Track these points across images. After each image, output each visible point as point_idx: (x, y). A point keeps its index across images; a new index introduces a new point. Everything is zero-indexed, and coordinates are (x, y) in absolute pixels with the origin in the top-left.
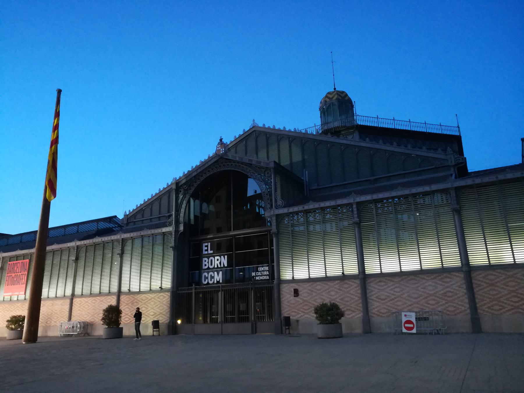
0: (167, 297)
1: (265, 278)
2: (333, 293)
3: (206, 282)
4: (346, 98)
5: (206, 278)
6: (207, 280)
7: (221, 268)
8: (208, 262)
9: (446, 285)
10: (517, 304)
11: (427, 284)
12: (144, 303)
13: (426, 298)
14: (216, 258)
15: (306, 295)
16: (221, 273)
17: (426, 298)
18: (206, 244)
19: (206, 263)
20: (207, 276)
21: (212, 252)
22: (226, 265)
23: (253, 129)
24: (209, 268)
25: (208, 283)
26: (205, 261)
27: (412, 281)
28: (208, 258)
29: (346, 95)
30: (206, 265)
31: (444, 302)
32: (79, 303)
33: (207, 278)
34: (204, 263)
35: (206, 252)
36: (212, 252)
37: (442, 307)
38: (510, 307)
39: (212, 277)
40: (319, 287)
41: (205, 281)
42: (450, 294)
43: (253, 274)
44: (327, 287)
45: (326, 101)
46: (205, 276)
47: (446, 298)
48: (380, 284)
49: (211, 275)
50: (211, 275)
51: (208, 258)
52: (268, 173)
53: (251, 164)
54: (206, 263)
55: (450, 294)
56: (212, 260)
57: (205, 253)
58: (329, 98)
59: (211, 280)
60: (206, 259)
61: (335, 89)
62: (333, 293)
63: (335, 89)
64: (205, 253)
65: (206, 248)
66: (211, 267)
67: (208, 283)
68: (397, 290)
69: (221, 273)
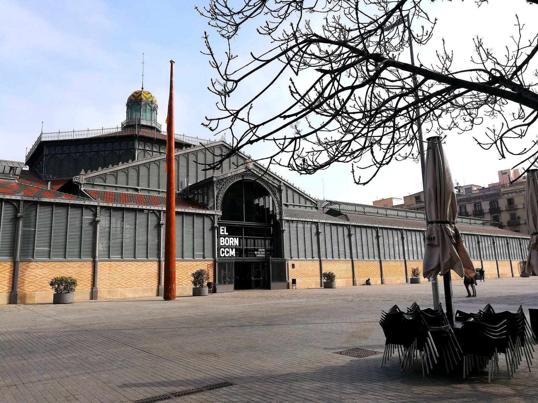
1: (263, 256)
3: (223, 255)
5: (223, 252)
12: (190, 269)
14: (231, 238)
16: (234, 250)
18: (223, 227)
19: (223, 241)
21: (227, 234)
22: (238, 245)
25: (225, 256)
28: (225, 238)
32: (108, 266)
33: (224, 252)
34: (221, 241)
35: (223, 234)
36: (227, 234)
39: (228, 252)
43: (256, 253)
51: (225, 238)
54: (223, 241)
57: (221, 233)
58: (145, 97)
60: (223, 238)
61: (142, 88)
62: (309, 267)
63: (142, 88)
64: (221, 233)
67: (225, 256)
69: (234, 250)
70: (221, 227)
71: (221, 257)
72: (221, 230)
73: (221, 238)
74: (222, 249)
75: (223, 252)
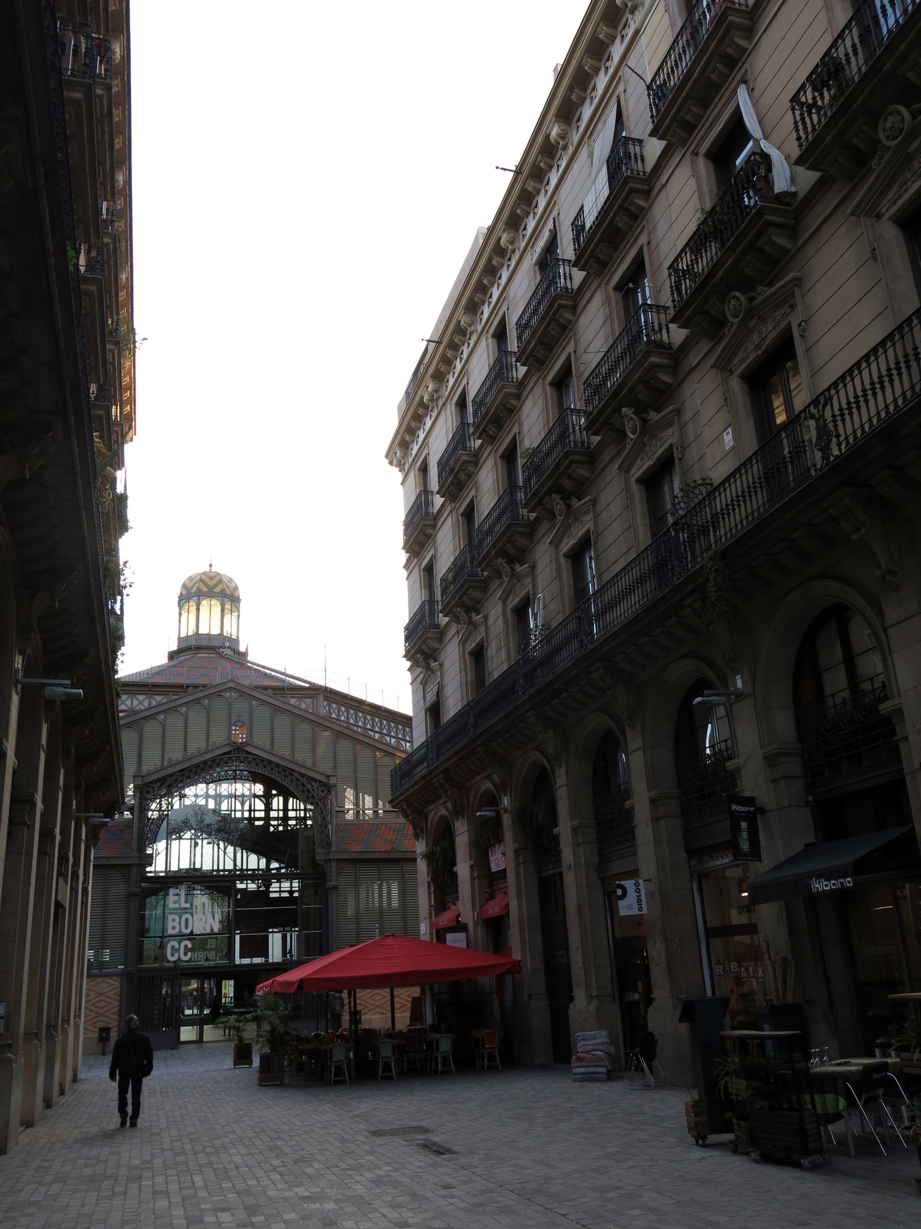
0: (118, 985)
3: (175, 958)
4: (236, 594)
5: (175, 950)
6: (176, 954)
8: (180, 923)
18: (177, 891)
20: (177, 946)
23: (231, 685)
26: (173, 920)
29: (236, 588)
30: (174, 928)
35: (177, 906)
41: (173, 955)
45: (199, 590)
46: (173, 947)
49: (186, 946)
50: (186, 946)
52: (323, 791)
53: (294, 771)
54: (176, 924)
56: (187, 920)
59: (185, 954)
60: (177, 918)
61: (211, 566)
63: (211, 566)
65: (176, 898)
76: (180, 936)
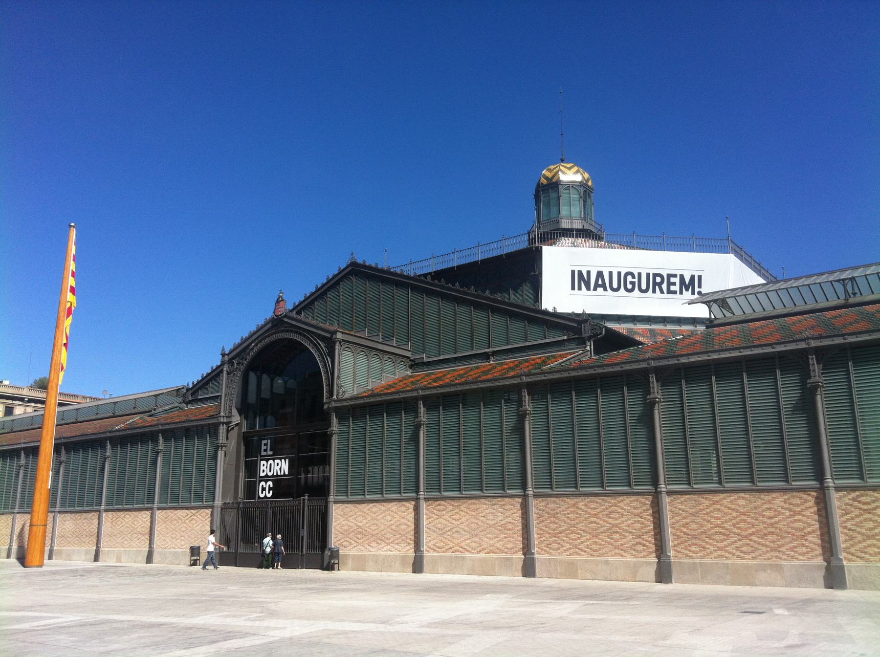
2: (389, 518)
3: (262, 496)
5: (264, 489)
7: (281, 476)
9: (507, 513)
10: (869, 542)
11: (487, 512)
13: (485, 530)
14: (277, 461)
15: (360, 518)
17: (485, 530)
21: (271, 453)
22: (287, 473)
24: (267, 476)
25: (266, 497)
27: (472, 507)
28: (267, 461)
31: (502, 536)
34: (262, 468)
36: (271, 453)
37: (502, 543)
38: (568, 546)
40: (374, 509)
42: (510, 526)
44: (383, 509)
47: (506, 531)
48: (439, 507)
51: (267, 461)
54: (264, 468)
55: (510, 526)
57: (263, 453)
64: (263, 453)
66: (270, 474)
67: (266, 497)
68: (457, 516)
70: (264, 442)
71: (259, 498)
72: (263, 447)
73: (263, 462)
74: (263, 483)
75: (264, 489)
76: (266, 478)
